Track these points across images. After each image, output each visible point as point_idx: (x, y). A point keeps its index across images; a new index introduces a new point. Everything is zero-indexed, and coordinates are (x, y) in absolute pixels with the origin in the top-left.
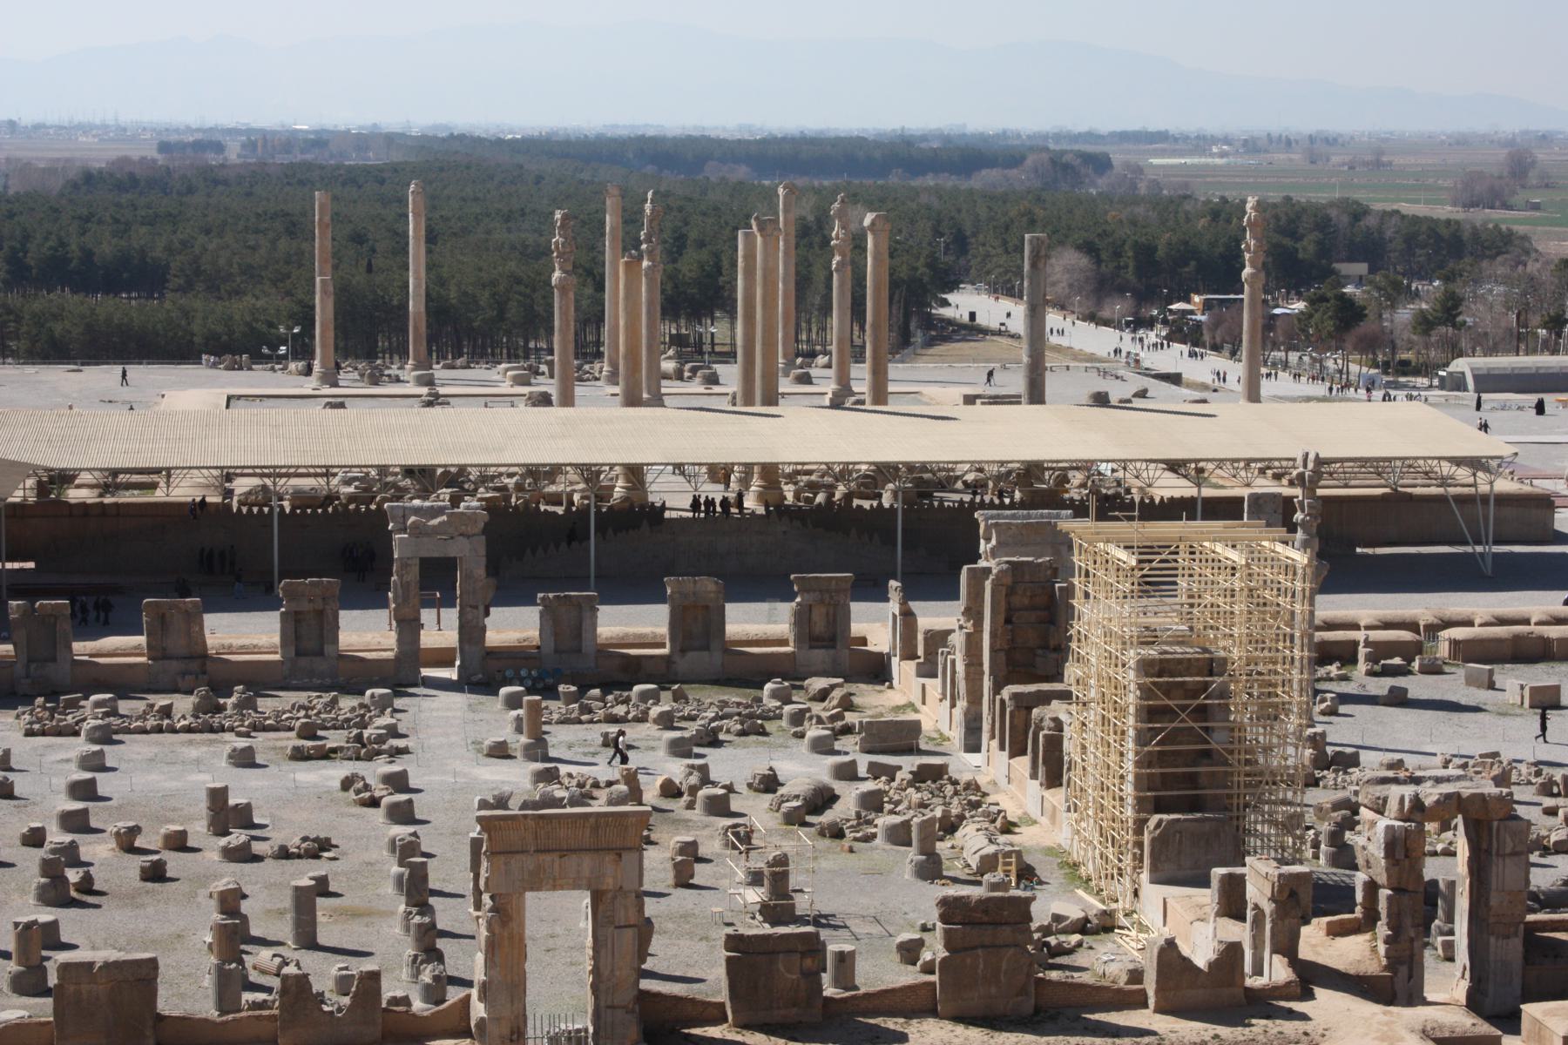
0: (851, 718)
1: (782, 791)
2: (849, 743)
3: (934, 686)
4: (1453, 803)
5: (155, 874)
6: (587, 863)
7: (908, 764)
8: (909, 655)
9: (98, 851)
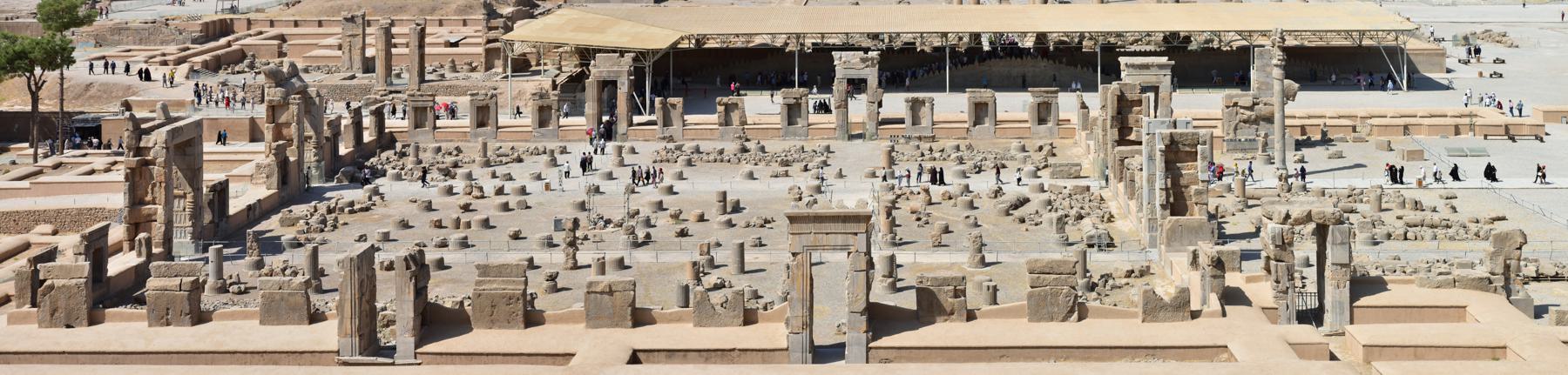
0: (1051, 160)
1: (1001, 199)
2: (1044, 174)
3: (1092, 143)
4: (1308, 218)
5: (683, 234)
6: (840, 240)
7: (1071, 184)
8: (1085, 128)
9: (663, 221)
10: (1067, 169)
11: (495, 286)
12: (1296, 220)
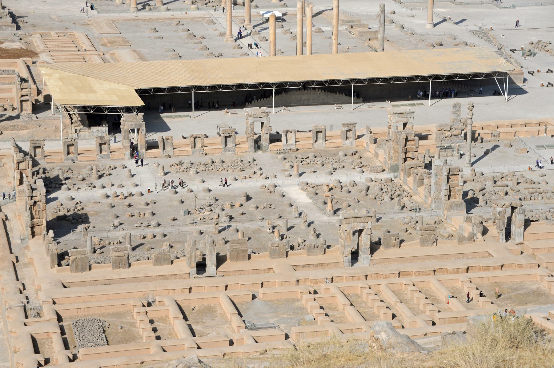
10: (376, 168)
11: (237, 247)
12: (507, 206)
